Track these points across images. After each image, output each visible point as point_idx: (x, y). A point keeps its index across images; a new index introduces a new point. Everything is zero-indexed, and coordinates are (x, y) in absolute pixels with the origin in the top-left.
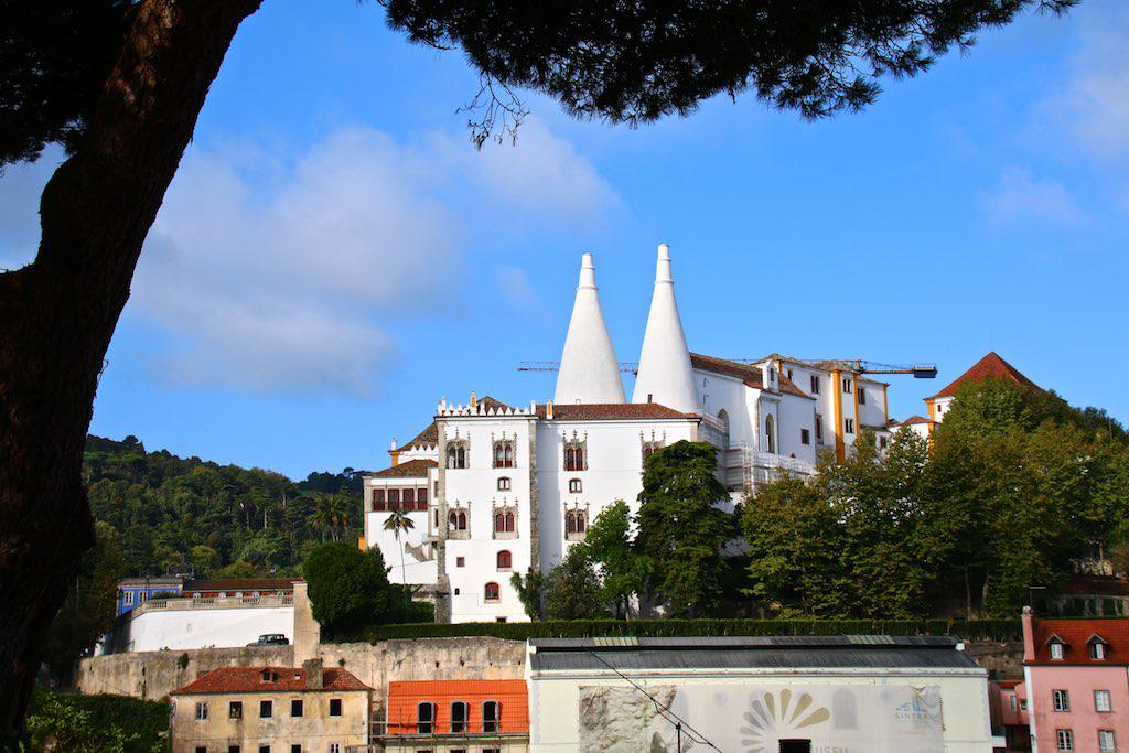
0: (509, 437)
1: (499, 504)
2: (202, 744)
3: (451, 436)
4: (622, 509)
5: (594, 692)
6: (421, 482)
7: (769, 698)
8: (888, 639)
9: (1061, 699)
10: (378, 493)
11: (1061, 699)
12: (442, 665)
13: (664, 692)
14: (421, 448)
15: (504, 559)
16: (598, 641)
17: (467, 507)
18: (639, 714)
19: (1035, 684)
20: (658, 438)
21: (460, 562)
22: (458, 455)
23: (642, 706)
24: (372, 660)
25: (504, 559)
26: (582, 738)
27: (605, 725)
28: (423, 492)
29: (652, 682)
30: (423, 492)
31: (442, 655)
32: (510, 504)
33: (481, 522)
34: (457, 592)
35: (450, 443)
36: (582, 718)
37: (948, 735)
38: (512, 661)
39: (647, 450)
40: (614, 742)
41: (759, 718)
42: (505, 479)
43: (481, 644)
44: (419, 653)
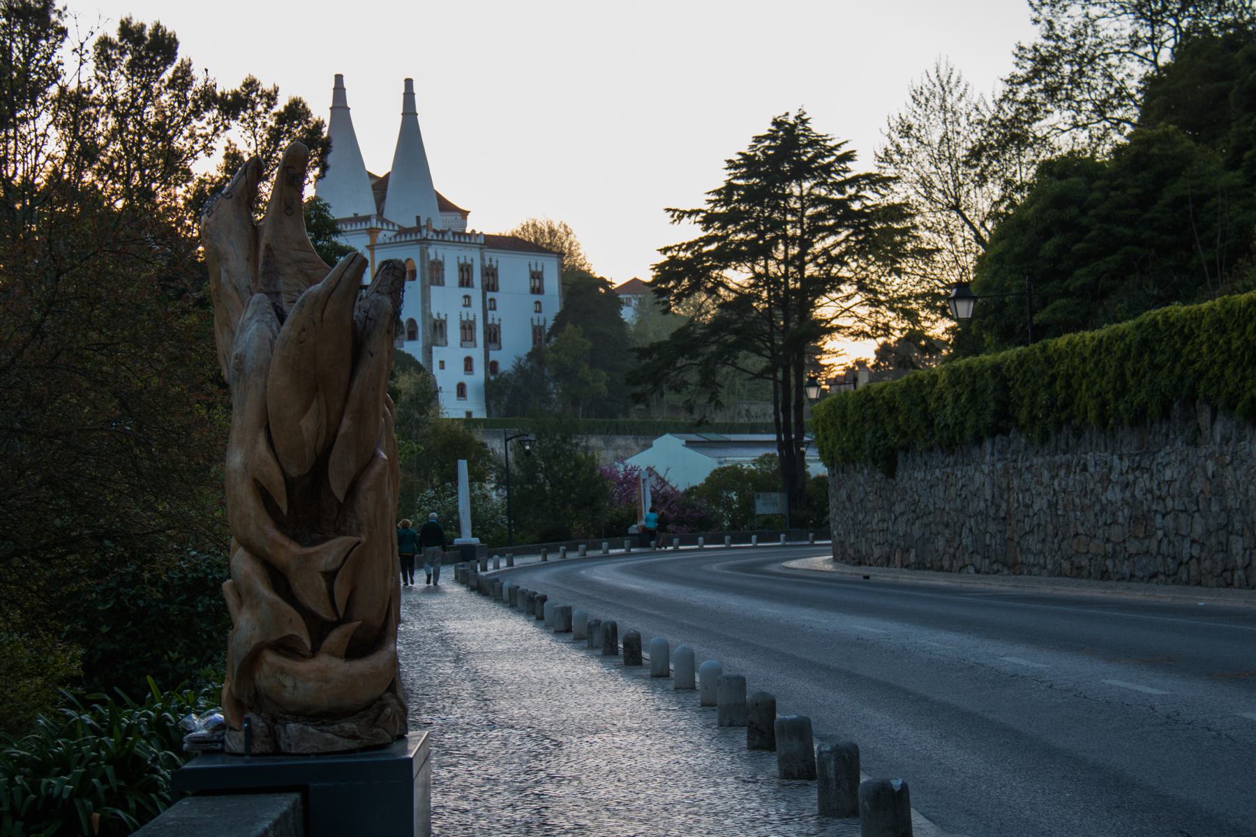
0: (469, 262)
1: (465, 318)
3: (432, 257)
15: (468, 364)
25: (468, 363)
32: (471, 318)
33: (454, 332)
35: (433, 263)
42: (466, 297)
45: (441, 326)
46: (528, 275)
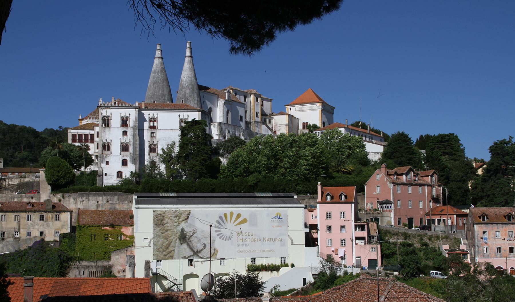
0: (127, 115)
1: (123, 141)
2: (3, 230)
3: (104, 114)
4: (173, 145)
5: (159, 212)
6: (92, 132)
7: (225, 215)
8: (269, 194)
9: (329, 215)
10: (74, 136)
11: (329, 215)
12: (100, 202)
13: (187, 213)
14: (91, 119)
15: (124, 163)
16: (161, 194)
17: (110, 141)
18: (176, 221)
19: (321, 210)
20: (186, 117)
21: (107, 163)
22: (106, 122)
23: (178, 218)
24: (72, 200)
26: (154, 230)
27: (163, 225)
28: (92, 136)
29: (181, 209)
30: (92, 136)
31: (100, 199)
32: (128, 141)
33: (116, 148)
34: (106, 174)
35: (104, 117)
36: (154, 222)
37: (289, 228)
38: (128, 201)
39: (181, 121)
40: (167, 231)
41: (222, 223)
43: (115, 195)
44: (90, 198)
45: (108, 146)
46: (178, 121)
